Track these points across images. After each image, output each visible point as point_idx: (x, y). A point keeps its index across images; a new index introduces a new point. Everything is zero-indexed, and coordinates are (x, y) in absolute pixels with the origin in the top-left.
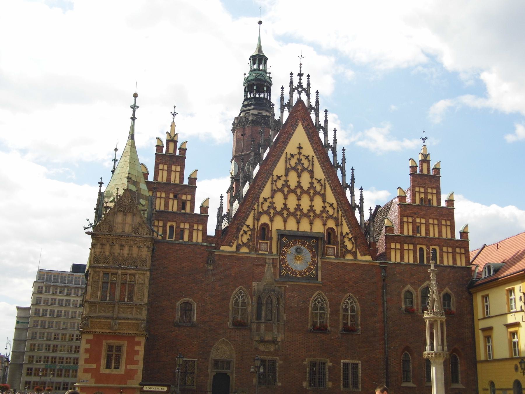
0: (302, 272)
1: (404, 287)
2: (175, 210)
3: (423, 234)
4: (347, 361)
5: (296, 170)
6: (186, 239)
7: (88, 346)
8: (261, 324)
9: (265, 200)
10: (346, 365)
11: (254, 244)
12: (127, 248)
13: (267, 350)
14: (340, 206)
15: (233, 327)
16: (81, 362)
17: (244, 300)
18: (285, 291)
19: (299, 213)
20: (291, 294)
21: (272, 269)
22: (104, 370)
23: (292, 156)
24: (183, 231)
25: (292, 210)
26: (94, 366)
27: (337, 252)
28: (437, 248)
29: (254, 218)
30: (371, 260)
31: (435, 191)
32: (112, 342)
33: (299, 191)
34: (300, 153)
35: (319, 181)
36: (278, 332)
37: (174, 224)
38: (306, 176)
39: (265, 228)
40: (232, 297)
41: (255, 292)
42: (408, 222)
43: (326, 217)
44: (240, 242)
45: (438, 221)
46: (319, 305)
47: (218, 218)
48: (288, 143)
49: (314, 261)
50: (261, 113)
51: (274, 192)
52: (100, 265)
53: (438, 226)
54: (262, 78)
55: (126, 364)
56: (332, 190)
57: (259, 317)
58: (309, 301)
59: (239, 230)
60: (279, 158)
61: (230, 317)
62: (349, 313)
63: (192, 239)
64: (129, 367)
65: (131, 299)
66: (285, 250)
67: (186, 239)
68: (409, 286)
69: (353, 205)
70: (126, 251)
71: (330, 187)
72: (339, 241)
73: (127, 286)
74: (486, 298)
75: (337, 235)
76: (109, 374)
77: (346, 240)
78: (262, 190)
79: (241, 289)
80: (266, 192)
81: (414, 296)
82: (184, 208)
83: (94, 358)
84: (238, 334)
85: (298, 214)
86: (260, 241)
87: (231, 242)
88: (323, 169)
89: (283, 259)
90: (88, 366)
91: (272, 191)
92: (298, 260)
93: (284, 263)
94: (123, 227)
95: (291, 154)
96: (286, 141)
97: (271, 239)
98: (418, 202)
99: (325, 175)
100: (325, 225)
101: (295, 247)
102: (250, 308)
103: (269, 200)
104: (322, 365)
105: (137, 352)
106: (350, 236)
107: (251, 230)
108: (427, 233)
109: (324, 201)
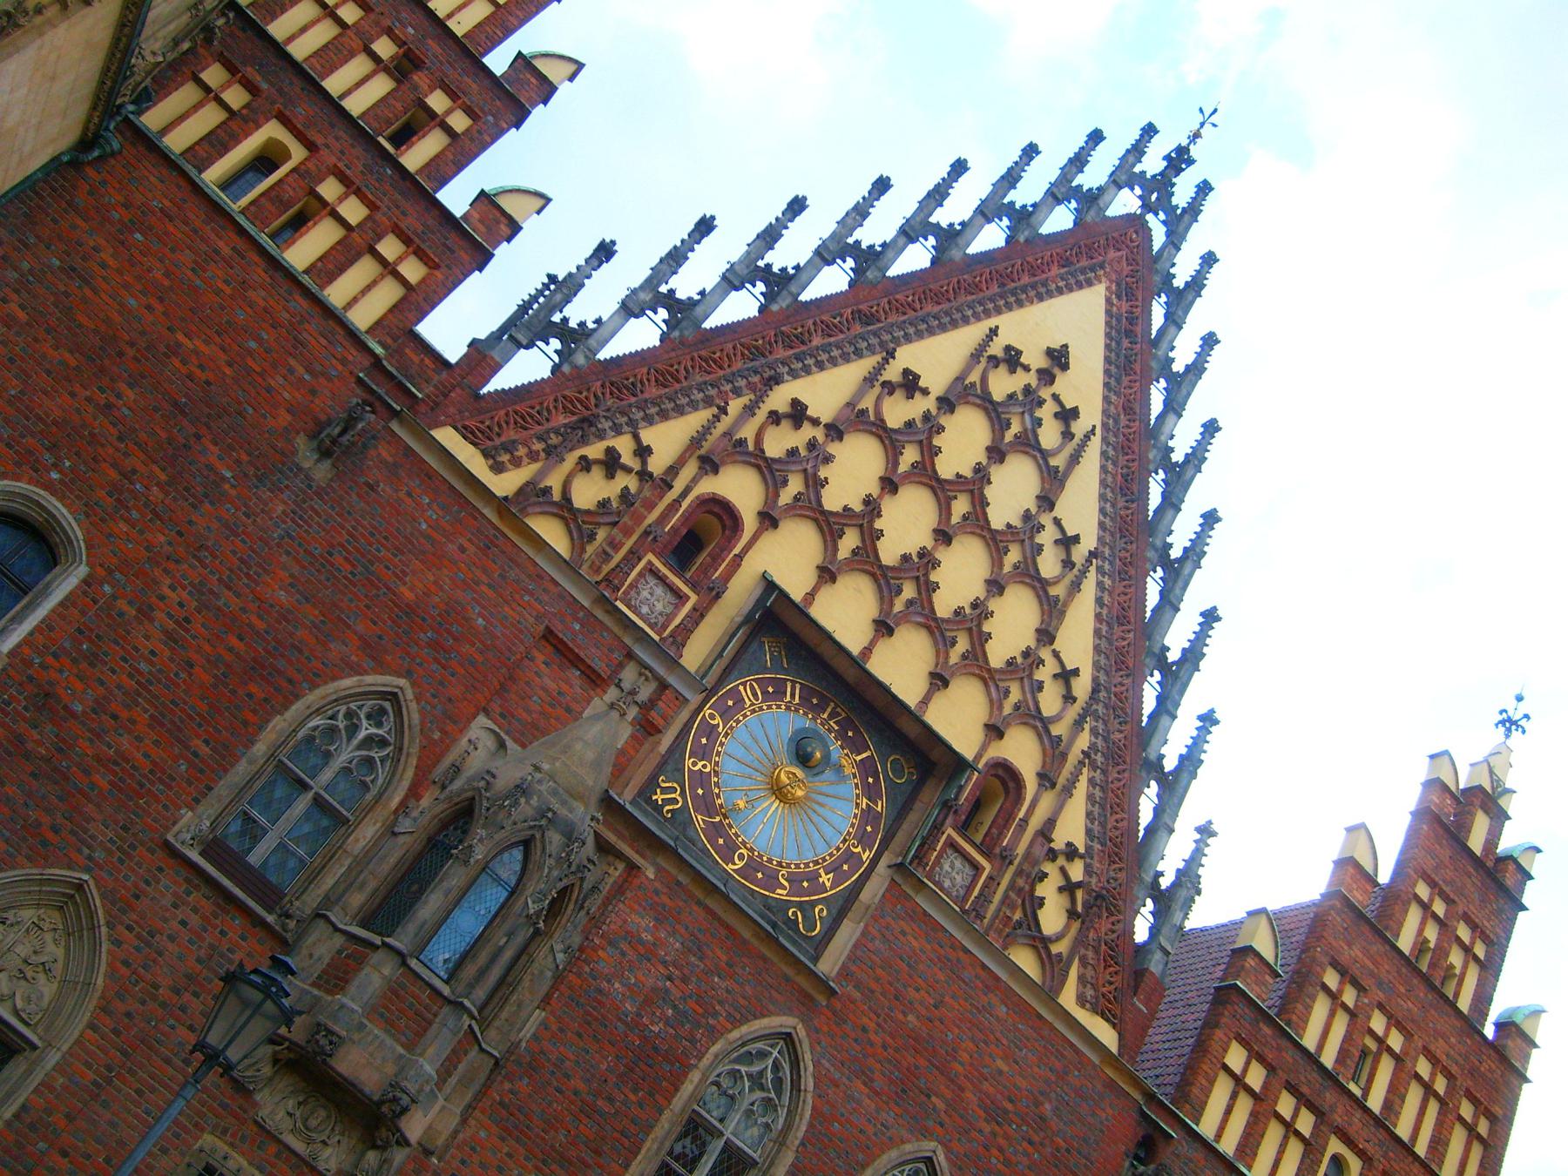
0: (760, 866)
3: (1375, 1102)
8: (379, 956)
9: (798, 414)
11: (617, 547)
13: (298, 1145)
14: (1100, 709)
15: (194, 855)
18: (620, 889)
20: (643, 924)
21: (625, 732)
23: (1012, 359)
27: (984, 897)
29: (696, 442)
30: (1114, 1050)
34: (1047, 377)
36: (445, 1072)
40: (313, 698)
41: (456, 769)
42: (1334, 996)
43: (1017, 707)
45: (1451, 1089)
47: (524, 308)
48: (1020, 304)
49: (849, 857)
53: (1442, 1113)
56: (1098, 617)
57: (390, 908)
58: (714, 1034)
59: (585, 428)
60: (954, 325)
61: (224, 789)
63: (331, 277)
66: (746, 694)
71: (1099, 601)
72: (1021, 849)
75: (1025, 821)
78: (807, 371)
79: (393, 697)
82: (404, 136)
84: (195, 921)
85: (904, 588)
86: (650, 557)
87: (509, 448)
88: (1102, 511)
89: (711, 732)
91: (850, 405)
92: (778, 791)
93: (703, 753)
96: (1014, 294)
97: (714, 594)
98: (1405, 943)
99: (1100, 539)
100: (995, 731)
101: (803, 721)
102: (367, 832)
106: (1077, 872)
107: (644, 475)
108: (1388, 1105)
109: (1046, 635)
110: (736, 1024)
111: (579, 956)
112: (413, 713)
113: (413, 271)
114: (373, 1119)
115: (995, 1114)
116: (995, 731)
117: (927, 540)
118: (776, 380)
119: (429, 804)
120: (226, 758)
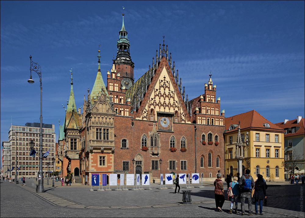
1: (202, 133)
2: (117, 103)
3: (209, 114)
4: (182, 160)
5: (164, 87)
6: (122, 115)
7: (92, 157)
9: (152, 99)
10: (182, 162)
12: (104, 119)
16: (90, 163)
17: (145, 138)
19: (165, 105)
21: (155, 127)
22: (99, 166)
23: (162, 81)
24: (121, 111)
25: (162, 104)
26: (95, 165)
28: (214, 119)
29: (148, 107)
31: (214, 97)
32: (100, 155)
33: (165, 96)
34: (165, 80)
35: (172, 92)
37: (117, 108)
38: (167, 89)
39: (152, 110)
44: (143, 116)
46: (172, 140)
49: (170, 124)
50: (126, 59)
51: (155, 96)
52: (95, 125)
54: (126, 42)
55: (108, 164)
57: (152, 145)
60: (157, 82)
62: (183, 143)
64: (108, 164)
65: (108, 139)
67: (122, 115)
68: (204, 133)
69: (185, 102)
70: (104, 119)
73: (106, 133)
74: (231, 137)
76: (102, 167)
77: (182, 115)
80: (152, 96)
81: (206, 137)
83: (95, 162)
85: (164, 105)
89: (159, 123)
90: (93, 165)
94: (103, 110)
95: (161, 80)
97: (155, 115)
100: (174, 110)
103: (154, 99)
104: (174, 162)
105: (111, 159)
108: (210, 113)
109: (174, 100)
110: (170, 137)
111: (161, 140)
112: (146, 135)
113: (128, 110)
114: (157, 155)
115: (185, 132)
116: (174, 110)
117: (164, 100)
118: (149, 98)
119: (150, 138)
120: (140, 143)
